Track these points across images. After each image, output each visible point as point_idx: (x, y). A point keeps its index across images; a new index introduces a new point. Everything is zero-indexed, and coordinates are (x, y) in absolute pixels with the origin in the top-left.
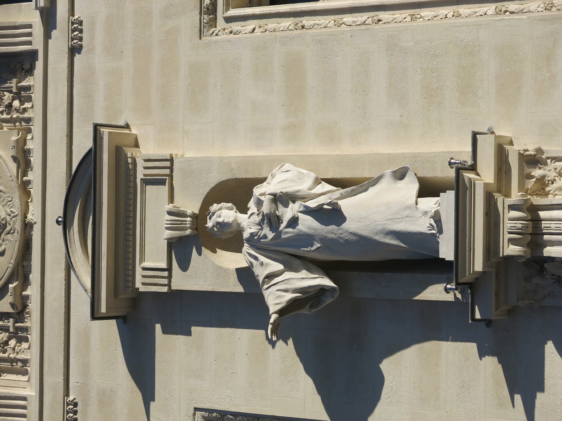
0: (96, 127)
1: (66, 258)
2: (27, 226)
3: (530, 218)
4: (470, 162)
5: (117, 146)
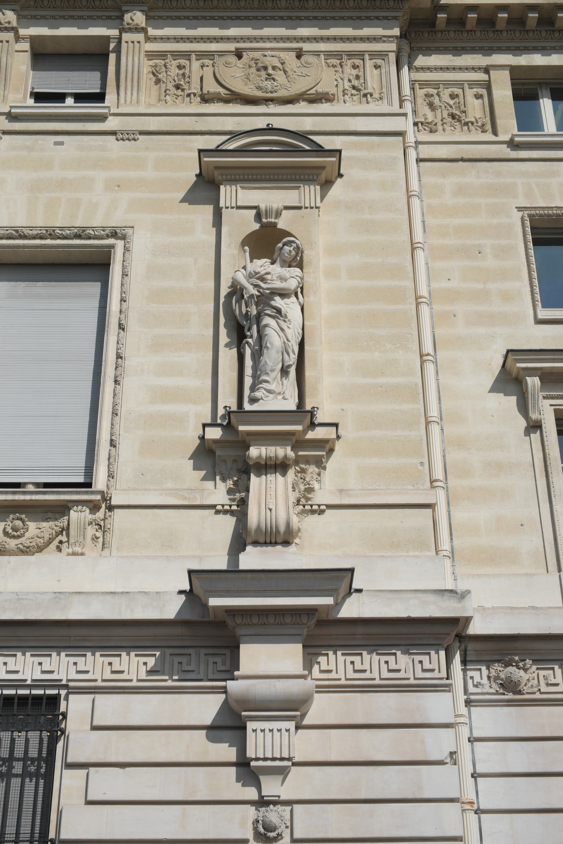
0: (340, 151)
2: (267, 101)
3: (277, 462)
4: (316, 422)
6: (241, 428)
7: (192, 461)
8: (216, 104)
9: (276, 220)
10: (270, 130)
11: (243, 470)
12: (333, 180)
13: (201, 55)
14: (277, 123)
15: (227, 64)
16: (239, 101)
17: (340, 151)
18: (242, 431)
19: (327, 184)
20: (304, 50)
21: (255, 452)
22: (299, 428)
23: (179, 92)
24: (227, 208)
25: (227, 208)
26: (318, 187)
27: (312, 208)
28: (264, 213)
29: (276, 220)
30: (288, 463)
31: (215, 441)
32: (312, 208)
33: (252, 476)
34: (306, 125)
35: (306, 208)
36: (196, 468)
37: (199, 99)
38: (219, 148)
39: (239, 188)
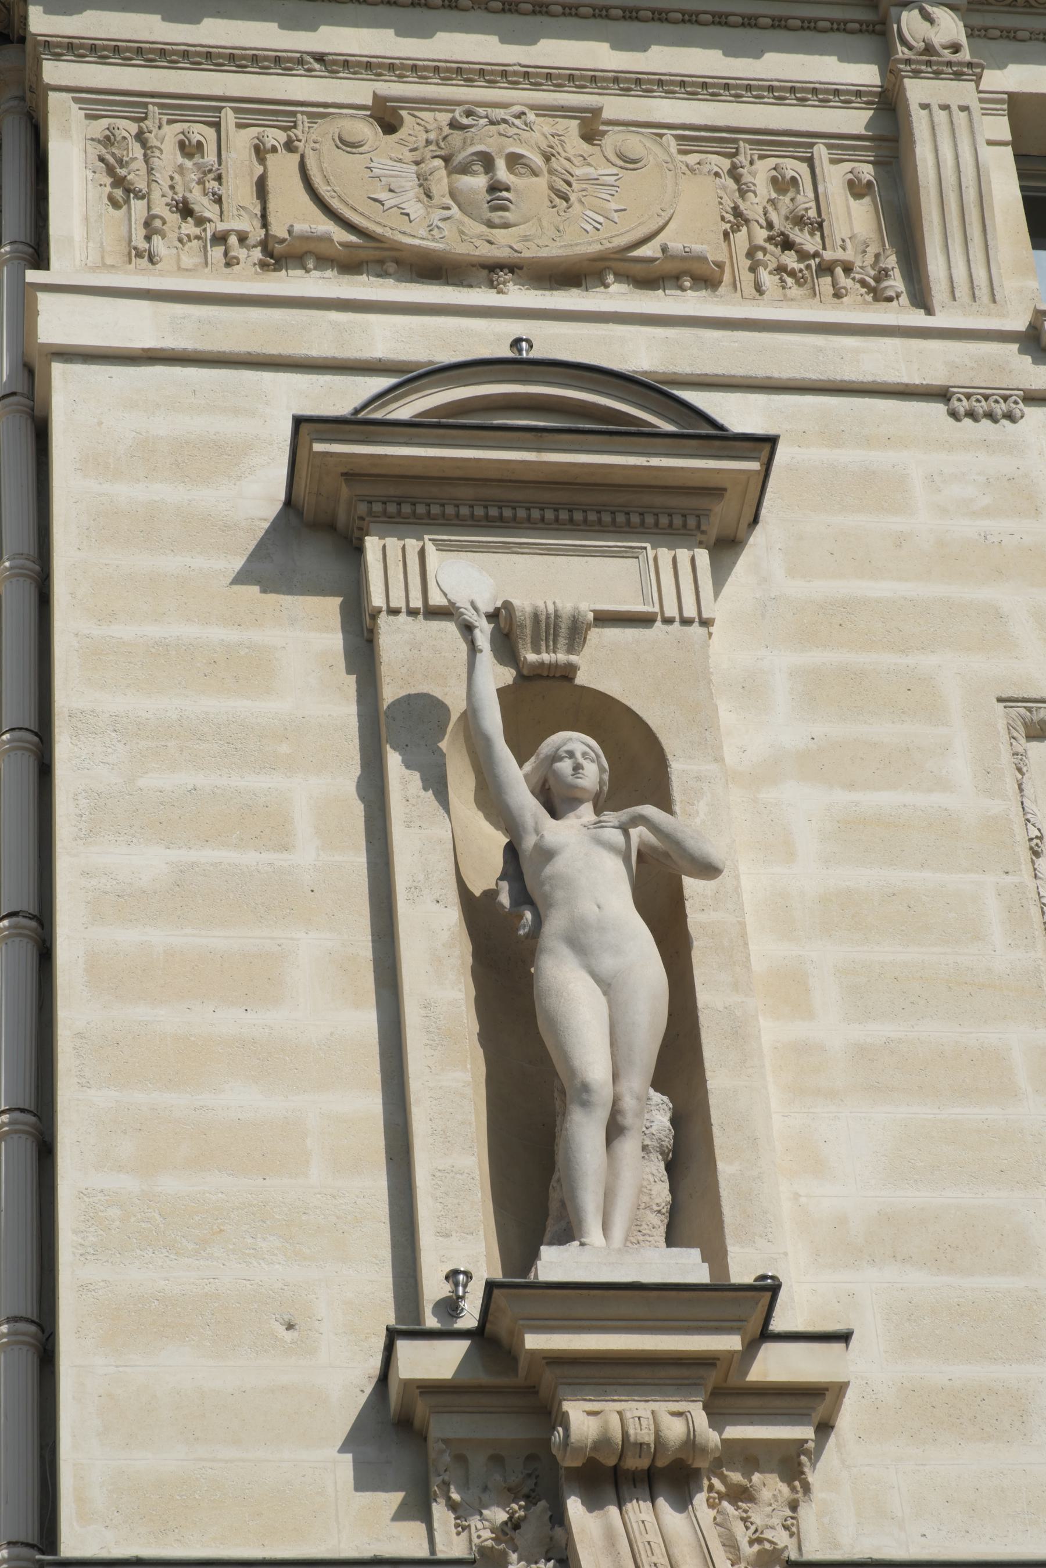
0: (771, 442)
1: (431, 363)
2: (491, 271)
5: (725, 490)
6: (534, 1341)
7: (349, 1457)
8: (315, 273)
9: (573, 658)
10: (517, 365)
11: (525, 1490)
12: (741, 534)
13: (255, 111)
14: (552, 342)
15: (348, 145)
16: (391, 267)
17: (771, 442)
18: (533, 1352)
19: (726, 547)
20: (606, 115)
21: (587, 1420)
22: (732, 1343)
23: (189, 228)
24: (394, 612)
25: (394, 612)
26: (703, 556)
27: (686, 622)
28: (528, 631)
29: (573, 658)
30: (695, 1465)
31: (430, 1389)
32: (686, 622)
33: (574, 1506)
34: (638, 353)
36: (361, 1484)
37: (257, 254)
39: (430, 548)
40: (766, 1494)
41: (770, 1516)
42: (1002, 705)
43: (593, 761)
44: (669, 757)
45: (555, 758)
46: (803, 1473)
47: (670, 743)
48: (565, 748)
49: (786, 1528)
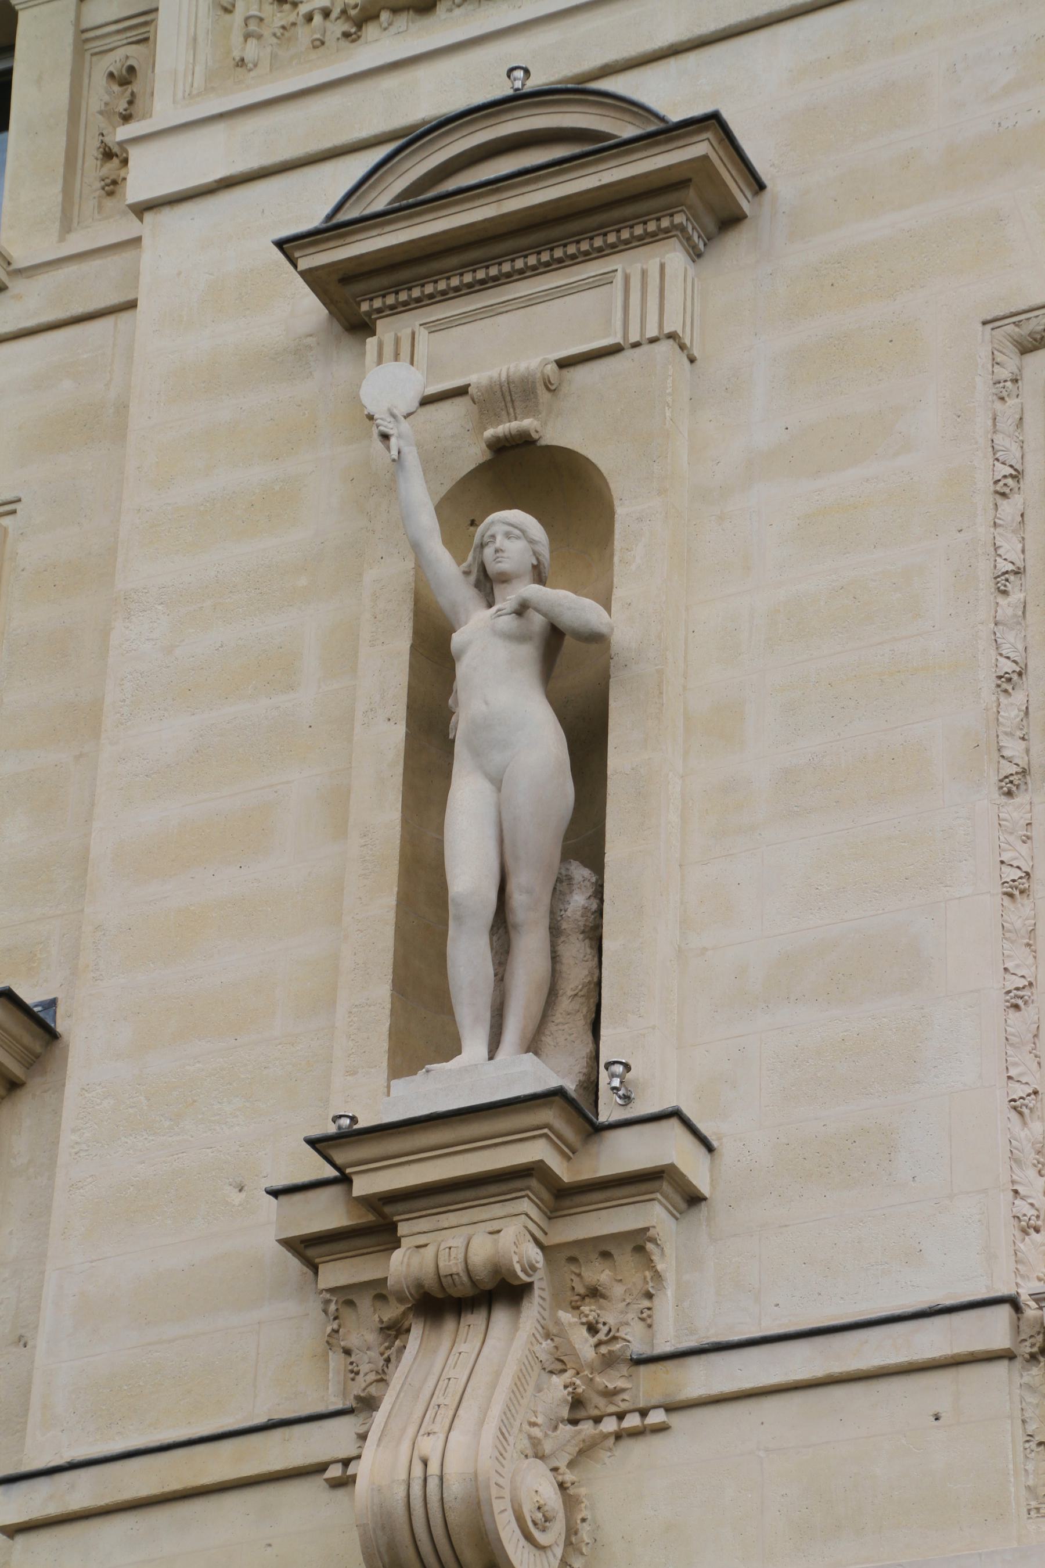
35: (636, 345)
38: (335, 221)
40: (618, 1290)
41: (624, 1312)
42: (989, 326)
43: (518, 538)
44: (616, 503)
45: (482, 546)
46: (652, 1261)
47: (619, 487)
48: (489, 533)
49: (643, 1320)
